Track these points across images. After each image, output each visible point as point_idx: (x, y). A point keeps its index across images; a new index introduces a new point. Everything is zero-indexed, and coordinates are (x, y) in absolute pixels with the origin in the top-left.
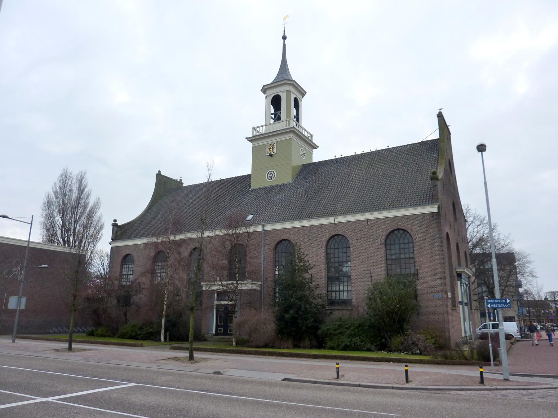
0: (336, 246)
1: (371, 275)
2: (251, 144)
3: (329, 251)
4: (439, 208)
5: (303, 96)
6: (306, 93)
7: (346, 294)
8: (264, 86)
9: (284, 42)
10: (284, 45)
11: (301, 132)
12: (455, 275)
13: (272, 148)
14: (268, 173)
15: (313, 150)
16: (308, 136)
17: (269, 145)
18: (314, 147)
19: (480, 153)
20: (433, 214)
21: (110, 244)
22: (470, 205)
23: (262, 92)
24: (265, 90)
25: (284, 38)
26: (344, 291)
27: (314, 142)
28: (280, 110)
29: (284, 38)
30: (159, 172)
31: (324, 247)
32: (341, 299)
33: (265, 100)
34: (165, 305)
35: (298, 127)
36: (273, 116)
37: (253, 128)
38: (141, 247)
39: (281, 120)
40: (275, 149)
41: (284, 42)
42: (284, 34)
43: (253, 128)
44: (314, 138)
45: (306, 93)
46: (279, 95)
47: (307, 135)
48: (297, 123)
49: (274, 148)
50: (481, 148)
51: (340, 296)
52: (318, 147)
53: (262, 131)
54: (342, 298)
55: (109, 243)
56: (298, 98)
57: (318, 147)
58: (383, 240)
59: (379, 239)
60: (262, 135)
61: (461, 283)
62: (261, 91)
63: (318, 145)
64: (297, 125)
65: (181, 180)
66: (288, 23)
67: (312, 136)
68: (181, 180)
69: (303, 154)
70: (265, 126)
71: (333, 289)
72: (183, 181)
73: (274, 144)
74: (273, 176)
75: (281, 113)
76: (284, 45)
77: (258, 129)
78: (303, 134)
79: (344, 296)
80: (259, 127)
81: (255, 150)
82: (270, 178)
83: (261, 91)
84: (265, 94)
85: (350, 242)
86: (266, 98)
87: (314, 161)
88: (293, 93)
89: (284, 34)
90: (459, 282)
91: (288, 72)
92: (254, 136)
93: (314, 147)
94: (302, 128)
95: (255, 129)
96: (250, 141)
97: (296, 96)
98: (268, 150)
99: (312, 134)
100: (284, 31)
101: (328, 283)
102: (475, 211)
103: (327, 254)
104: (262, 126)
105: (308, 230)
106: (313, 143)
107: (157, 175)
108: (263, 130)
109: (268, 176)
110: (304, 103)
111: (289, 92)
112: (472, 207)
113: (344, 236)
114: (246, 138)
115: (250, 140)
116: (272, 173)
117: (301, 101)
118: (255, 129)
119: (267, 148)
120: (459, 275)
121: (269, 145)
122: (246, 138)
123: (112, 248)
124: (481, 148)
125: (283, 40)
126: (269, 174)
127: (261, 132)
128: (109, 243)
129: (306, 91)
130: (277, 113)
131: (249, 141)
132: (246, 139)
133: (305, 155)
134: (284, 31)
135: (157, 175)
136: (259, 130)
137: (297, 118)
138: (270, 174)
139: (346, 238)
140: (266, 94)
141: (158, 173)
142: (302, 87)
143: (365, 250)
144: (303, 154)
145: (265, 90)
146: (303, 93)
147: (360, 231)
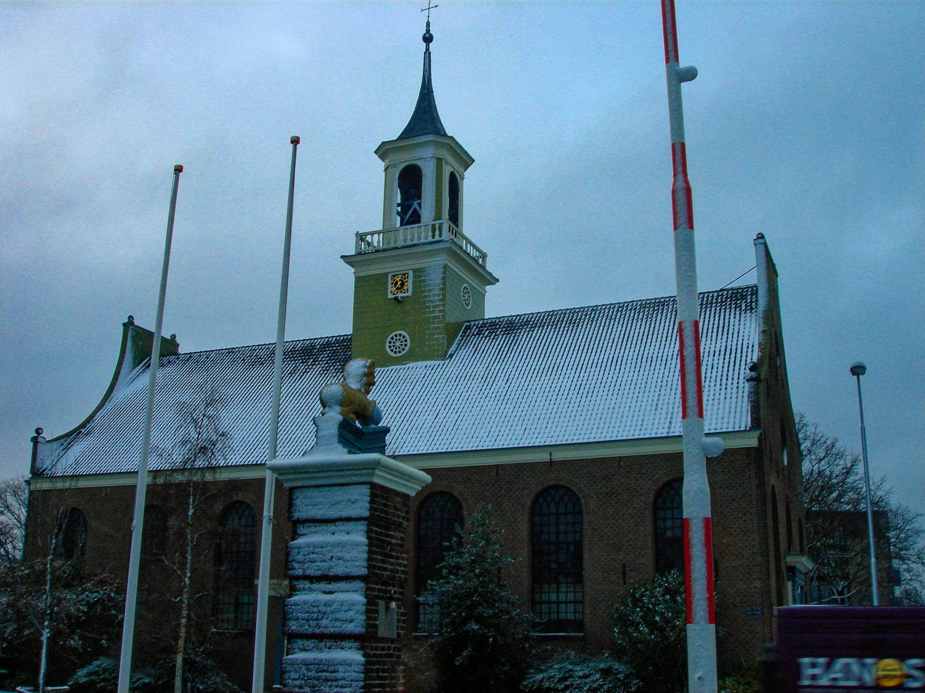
0: (553, 510)
1: (624, 570)
2: (353, 270)
3: (537, 519)
4: (760, 440)
5: (467, 166)
6: (474, 161)
7: (571, 608)
8: (383, 143)
9: (427, 49)
10: (428, 54)
11: (461, 245)
12: (784, 569)
13: (401, 284)
14: (392, 338)
15: (487, 287)
16: (478, 255)
17: (394, 276)
18: (492, 280)
19: (856, 377)
20: (748, 450)
21: (28, 483)
22: (805, 415)
23: (376, 156)
24: (383, 151)
25: (428, 39)
26: (566, 603)
27: (490, 271)
28: (419, 197)
29: (428, 39)
31: (527, 510)
32: (560, 618)
33: (384, 173)
34: (184, 626)
35: (456, 236)
36: (399, 209)
37: (357, 234)
38: (103, 494)
39: (422, 220)
40: (409, 285)
41: (427, 49)
43: (357, 234)
44: (488, 259)
45: (474, 161)
46: (417, 166)
47: (474, 253)
48: (452, 225)
49: (406, 284)
50: (858, 370)
51: (558, 613)
52: (498, 280)
53: (379, 242)
54: (563, 616)
55: (26, 481)
56: (456, 173)
57: (498, 280)
58: (651, 500)
59: (643, 498)
60: (377, 251)
61: (793, 586)
62: (375, 152)
63: (497, 277)
64: (451, 228)
65: (174, 336)
66: (436, 6)
67: (484, 256)
68: (174, 336)
69: (466, 296)
70: (383, 232)
71: (545, 597)
72: (178, 340)
73: (405, 274)
74: (402, 345)
75: (420, 205)
76: (428, 54)
77: (369, 238)
78: (461, 248)
79: (568, 613)
80: (372, 234)
81: (360, 282)
82: (396, 348)
83: (375, 152)
84: (383, 160)
85: (583, 501)
86: (386, 170)
88: (447, 163)
90: (789, 584)
91: (435, 116)
92: (360, 254)
93: (492, 280)
94: (464, 237)
95: (361, 237)
97: (452, 170)
98: (391, 288)
99: (485, 252)
100: (428, 24)
101: (535, 585)
102: (816, 428)
103: (532, 524)
104: (378, 233)
105: (493, 473)
106: (487, 272)
107: (124, 325)
108: (376, 240)
109: (392, 344)
110: (470, 182)
111: (439, 161)
112: (808, 419)
113: (568, 489)
114: (342, 257)
116: (400, 339)
117: (463, 179)
118: (361, 237)
119: (390, 282)
120: (792, 570)
121: (394, 276)
122: (342, 257)
123: (31, 493)
124: (858, 370)
125: (425, 44)
126: (401, 349)
127: (376, 244)
128: (26, 481)
129: (474, 157)
130: (415, 208)
131: (348, 263)
132: (341, 260)
133: (462, 294)
134: (428, 24)
135: (124, 325)
136: (370, 241)
137: (455, 217)
138: (396, 340)
139: (574, 493)
140: (387, 161)
141: (126, 321)
142: (466, 149)
143: (614, 519)
144: (466, 296)
145: (383, 151)
146: (466, 161)
147: (604, 479)
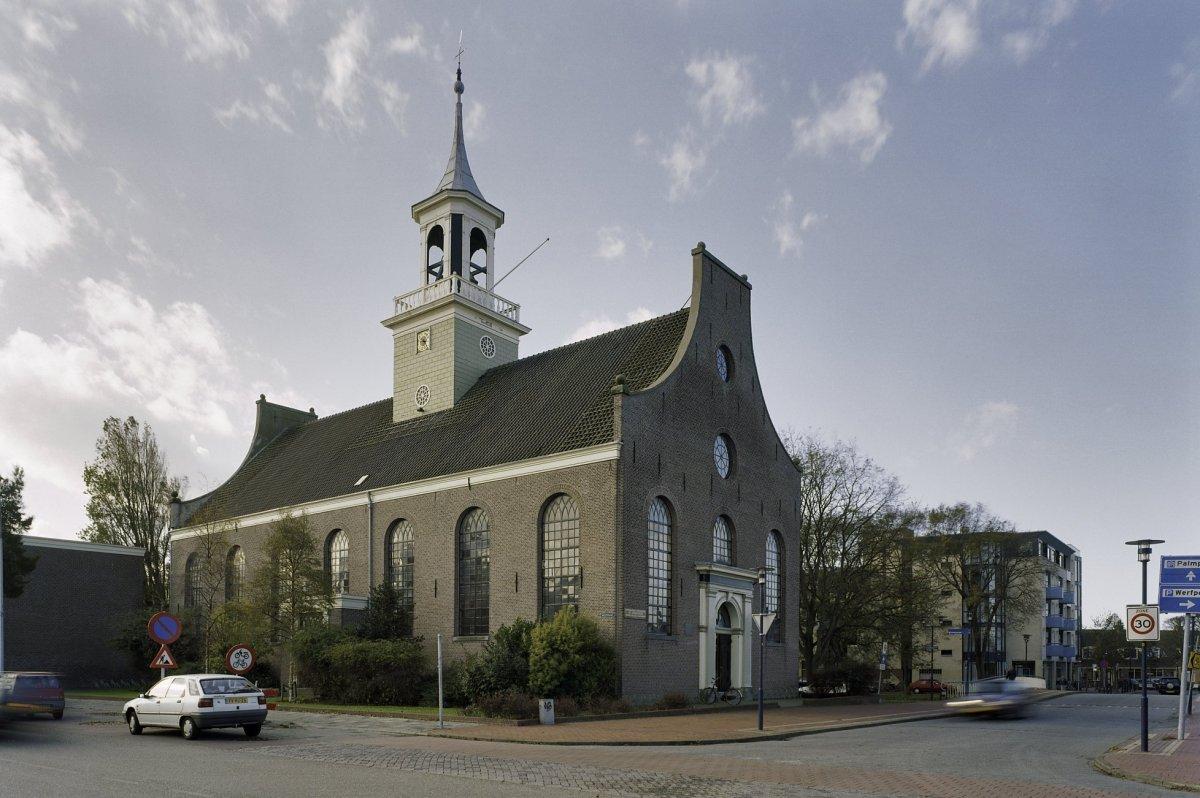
9: (459, 99)
10: (459, 105)
25: (459, 89)
30: (263, 397)
41: (459, 99)
42: (459, 78)
76: (459, 105)
87: (520, 358)
89: (459, 78)
96: (391, 326)
107: (258, 403)
108: (416, 302)
115: (392, 324)
135: (258, 403)
141: (260, 399)
145: (418, 212)
